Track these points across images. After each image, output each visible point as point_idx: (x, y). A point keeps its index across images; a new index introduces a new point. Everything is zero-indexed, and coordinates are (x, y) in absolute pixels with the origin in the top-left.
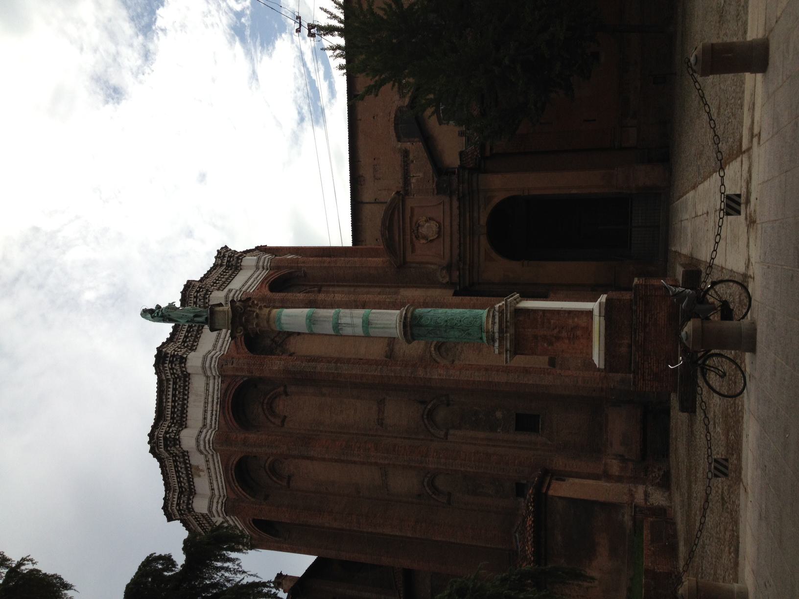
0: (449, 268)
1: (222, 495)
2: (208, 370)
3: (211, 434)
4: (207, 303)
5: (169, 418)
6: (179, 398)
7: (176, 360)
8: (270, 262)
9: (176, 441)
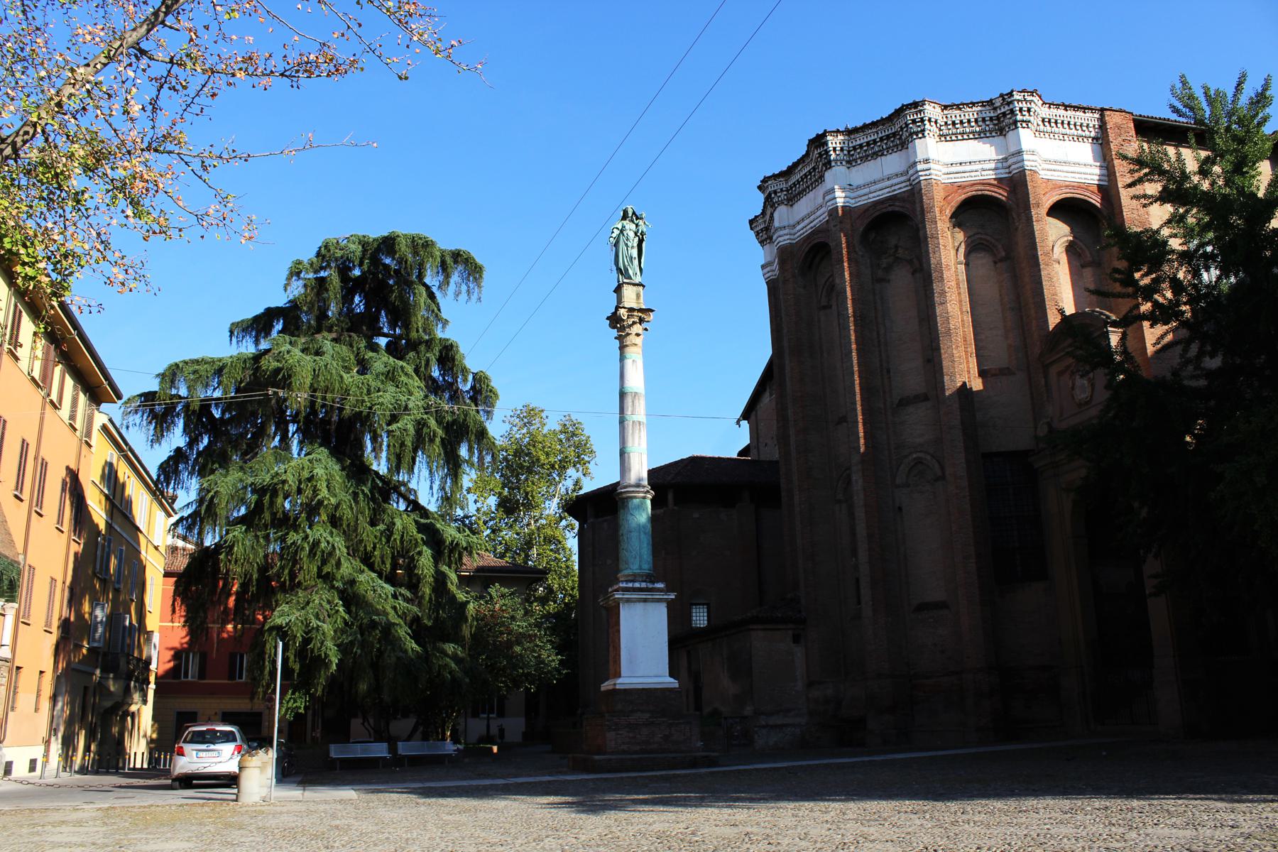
9: (774, 207)
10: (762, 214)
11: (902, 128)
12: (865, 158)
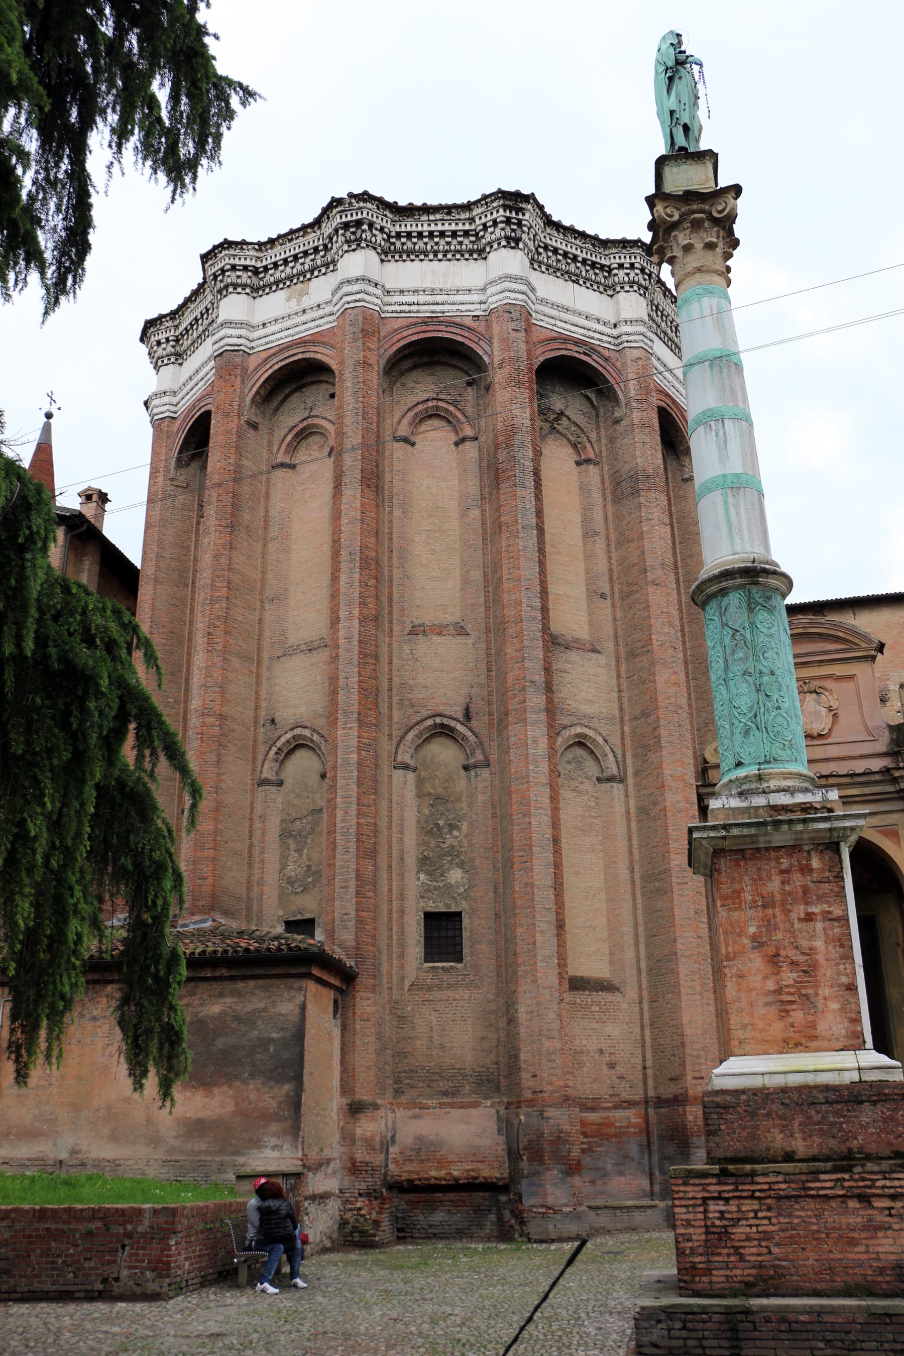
1: (253, 344)
4: (622, 288)
5: (398, 229)
6: (437, 244)
7: (513, 230)
9: (356, 243)
10: (260, 244)
12: (555, 271)
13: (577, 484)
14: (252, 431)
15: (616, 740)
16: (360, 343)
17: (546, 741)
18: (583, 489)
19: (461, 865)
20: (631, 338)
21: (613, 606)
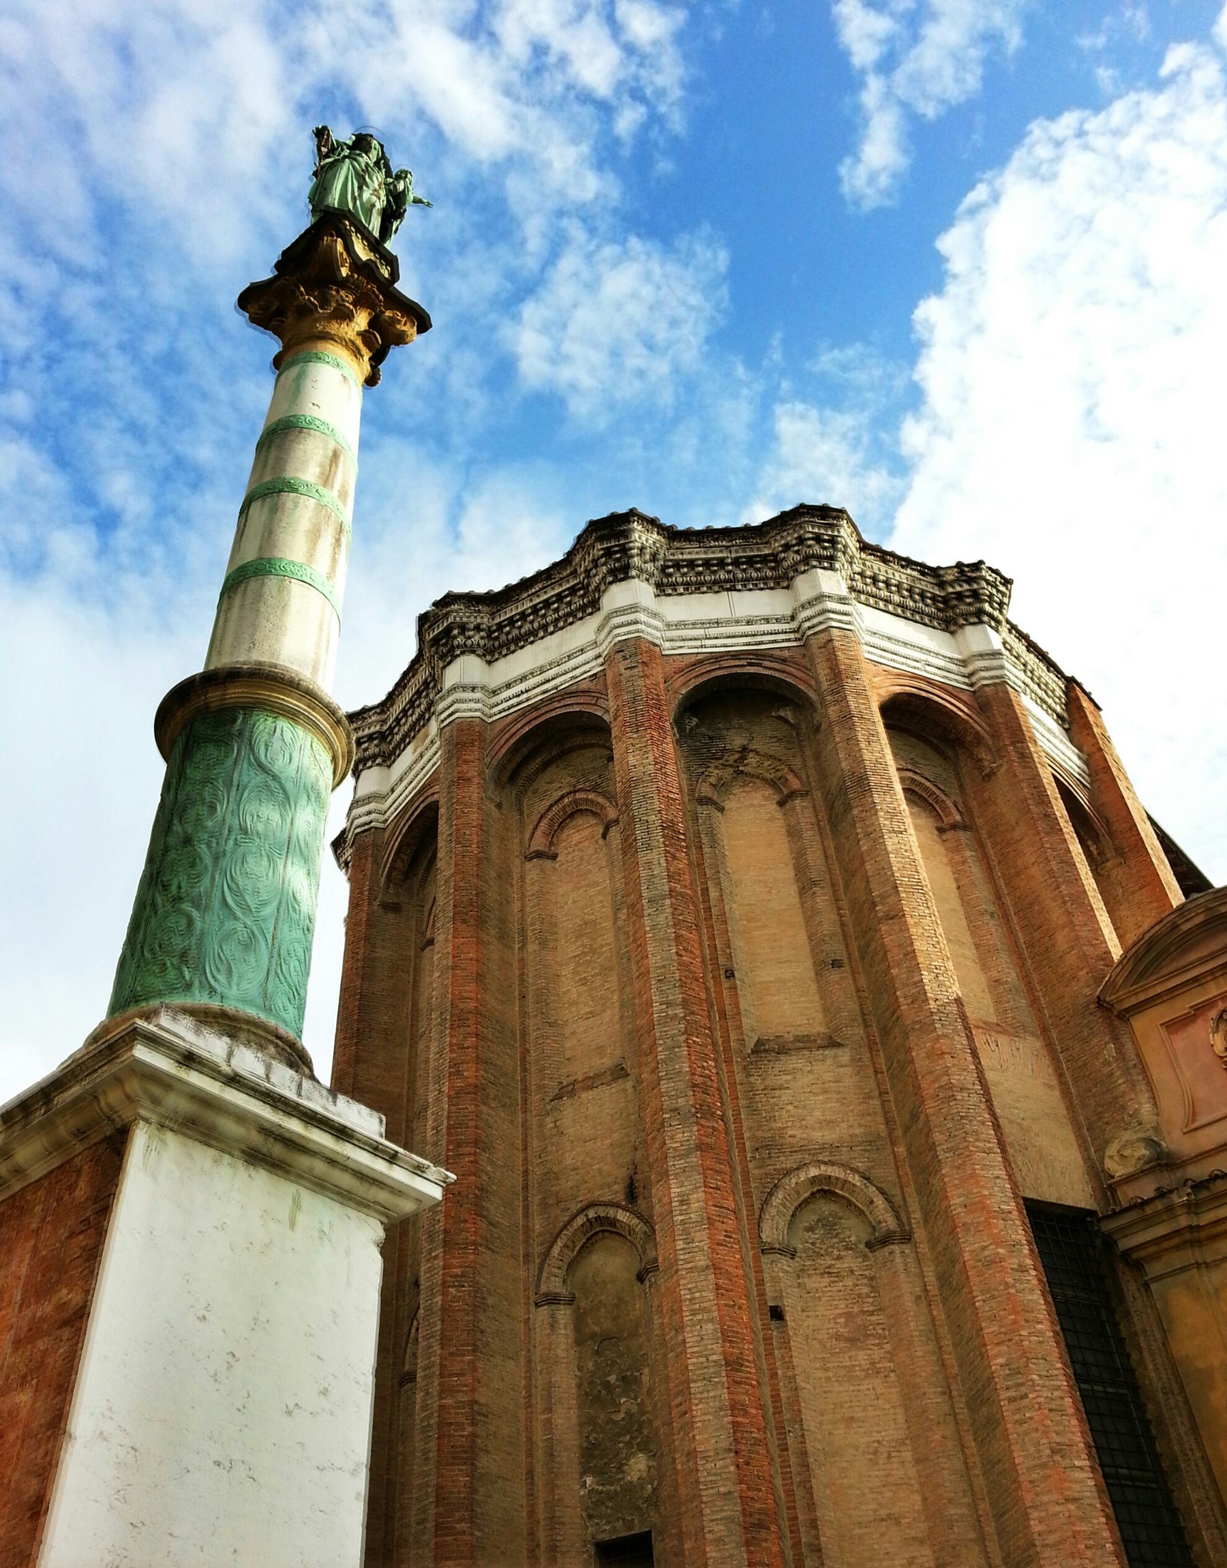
0: (1163, 1161)
2: (607, 629)
3: (470, 710)
4: (796, 570)
5: (497, 620)
6: (544, 616)
7: (618, 560)
8: (994, 684)
9: (450, 656)
11: (787, 547)
12: (695, 587)
13: (783, 830)
14: (391, 916)
15: (886, 1174)
16: (454, 760)
17: (701, 1195)
18: (793, 833)
19: (644, 1447)
20: (815, 621)
21: (853, 973)
